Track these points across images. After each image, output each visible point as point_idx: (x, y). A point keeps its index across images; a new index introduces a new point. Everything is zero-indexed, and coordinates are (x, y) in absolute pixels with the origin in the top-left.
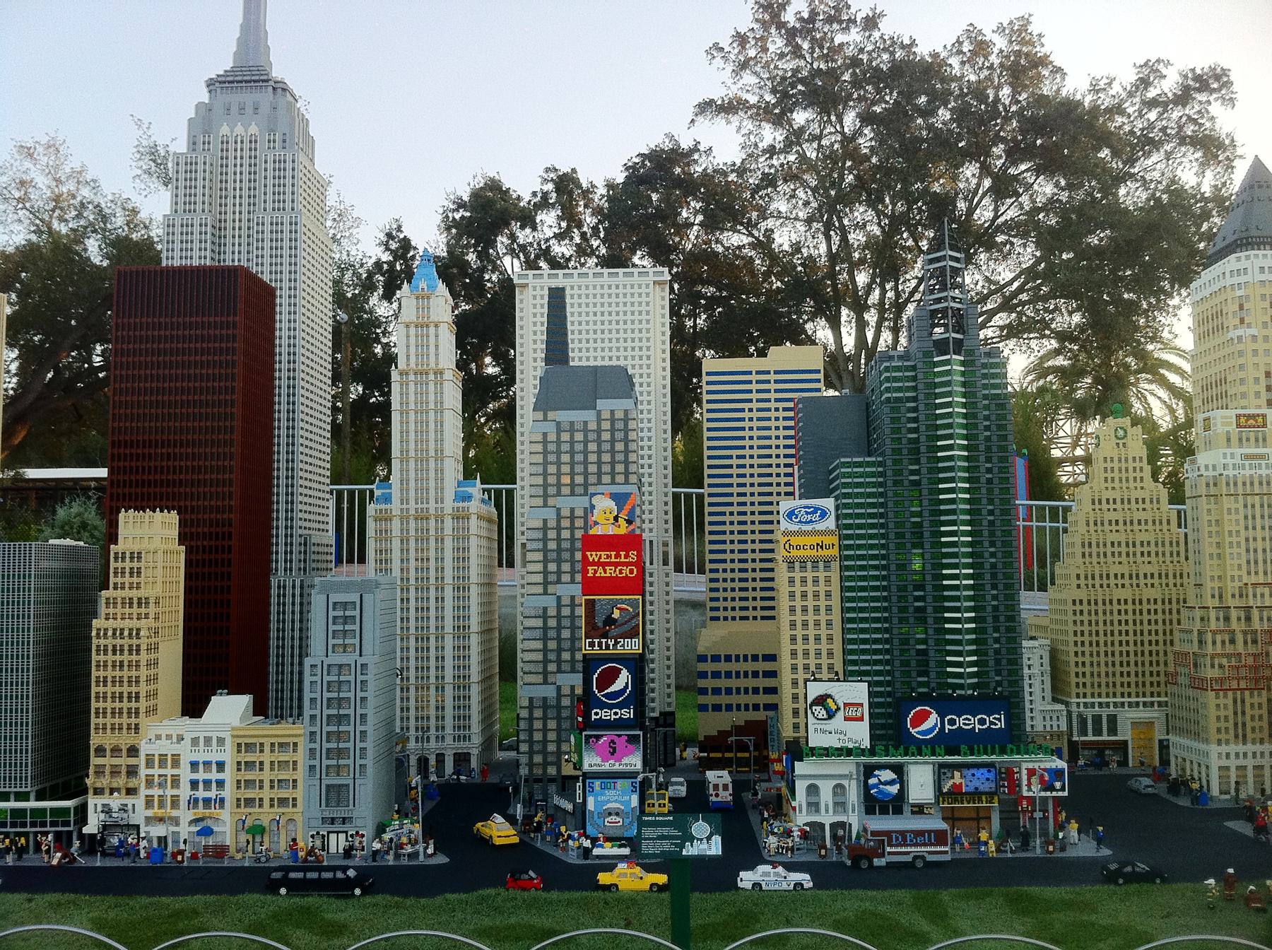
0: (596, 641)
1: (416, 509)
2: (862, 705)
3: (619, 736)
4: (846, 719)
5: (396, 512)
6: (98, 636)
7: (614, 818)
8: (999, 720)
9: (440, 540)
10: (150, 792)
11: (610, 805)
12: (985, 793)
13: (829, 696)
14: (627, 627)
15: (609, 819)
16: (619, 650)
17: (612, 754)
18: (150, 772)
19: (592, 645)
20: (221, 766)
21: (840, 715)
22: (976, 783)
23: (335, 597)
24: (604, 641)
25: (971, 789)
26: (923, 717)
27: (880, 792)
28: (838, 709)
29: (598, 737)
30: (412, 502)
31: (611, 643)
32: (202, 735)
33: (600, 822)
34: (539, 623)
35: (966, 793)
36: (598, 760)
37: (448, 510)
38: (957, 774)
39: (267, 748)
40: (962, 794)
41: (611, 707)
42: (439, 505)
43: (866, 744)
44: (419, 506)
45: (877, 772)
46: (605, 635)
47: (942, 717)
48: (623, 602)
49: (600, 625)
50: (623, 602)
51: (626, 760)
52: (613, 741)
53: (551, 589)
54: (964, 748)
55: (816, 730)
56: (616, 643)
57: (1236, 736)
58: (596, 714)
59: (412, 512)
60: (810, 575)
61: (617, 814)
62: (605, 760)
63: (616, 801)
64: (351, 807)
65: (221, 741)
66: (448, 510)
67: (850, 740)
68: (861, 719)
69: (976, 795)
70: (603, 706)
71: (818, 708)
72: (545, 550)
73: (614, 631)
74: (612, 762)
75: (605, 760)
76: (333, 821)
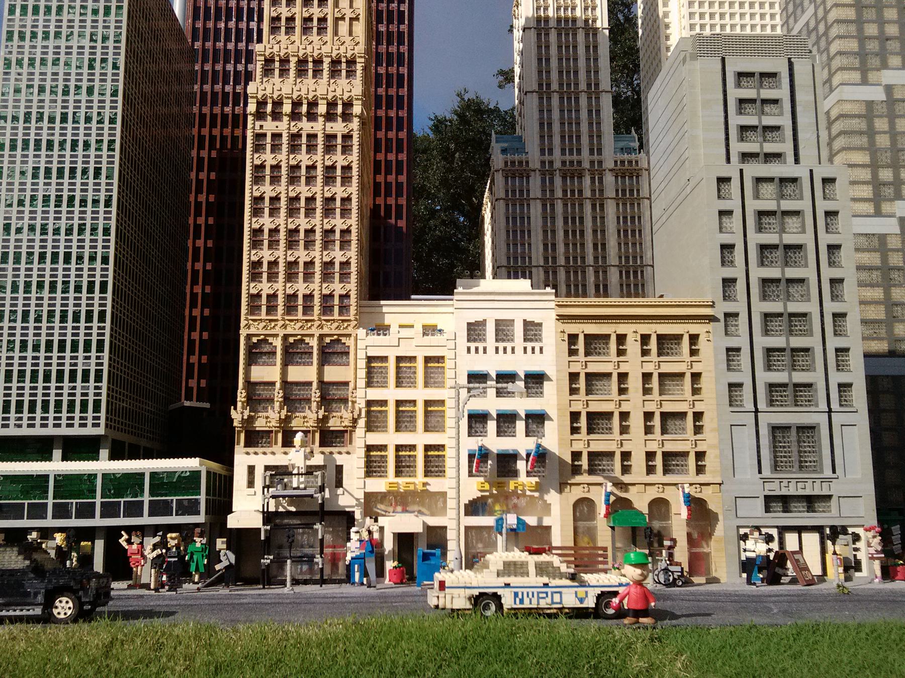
1: (564, 163)
5: (535, 164)
6: (260, 115)
9: (598, 203)
10: (375, 438)
18: (375, 394)
20: (535, 380)
23: (735, 65)
30: (557, 152)
32: (491, 317)
34: (874, 259)
37: (609, 164)
39: (633, 346)
42: (596, 157)
44: (568, 157)
53: (886, 207)
59: (557, 165)
64: (828, 472)
65: (532, 330)
66: (609, 164)
72: (872, 149)
76: (786, 502)
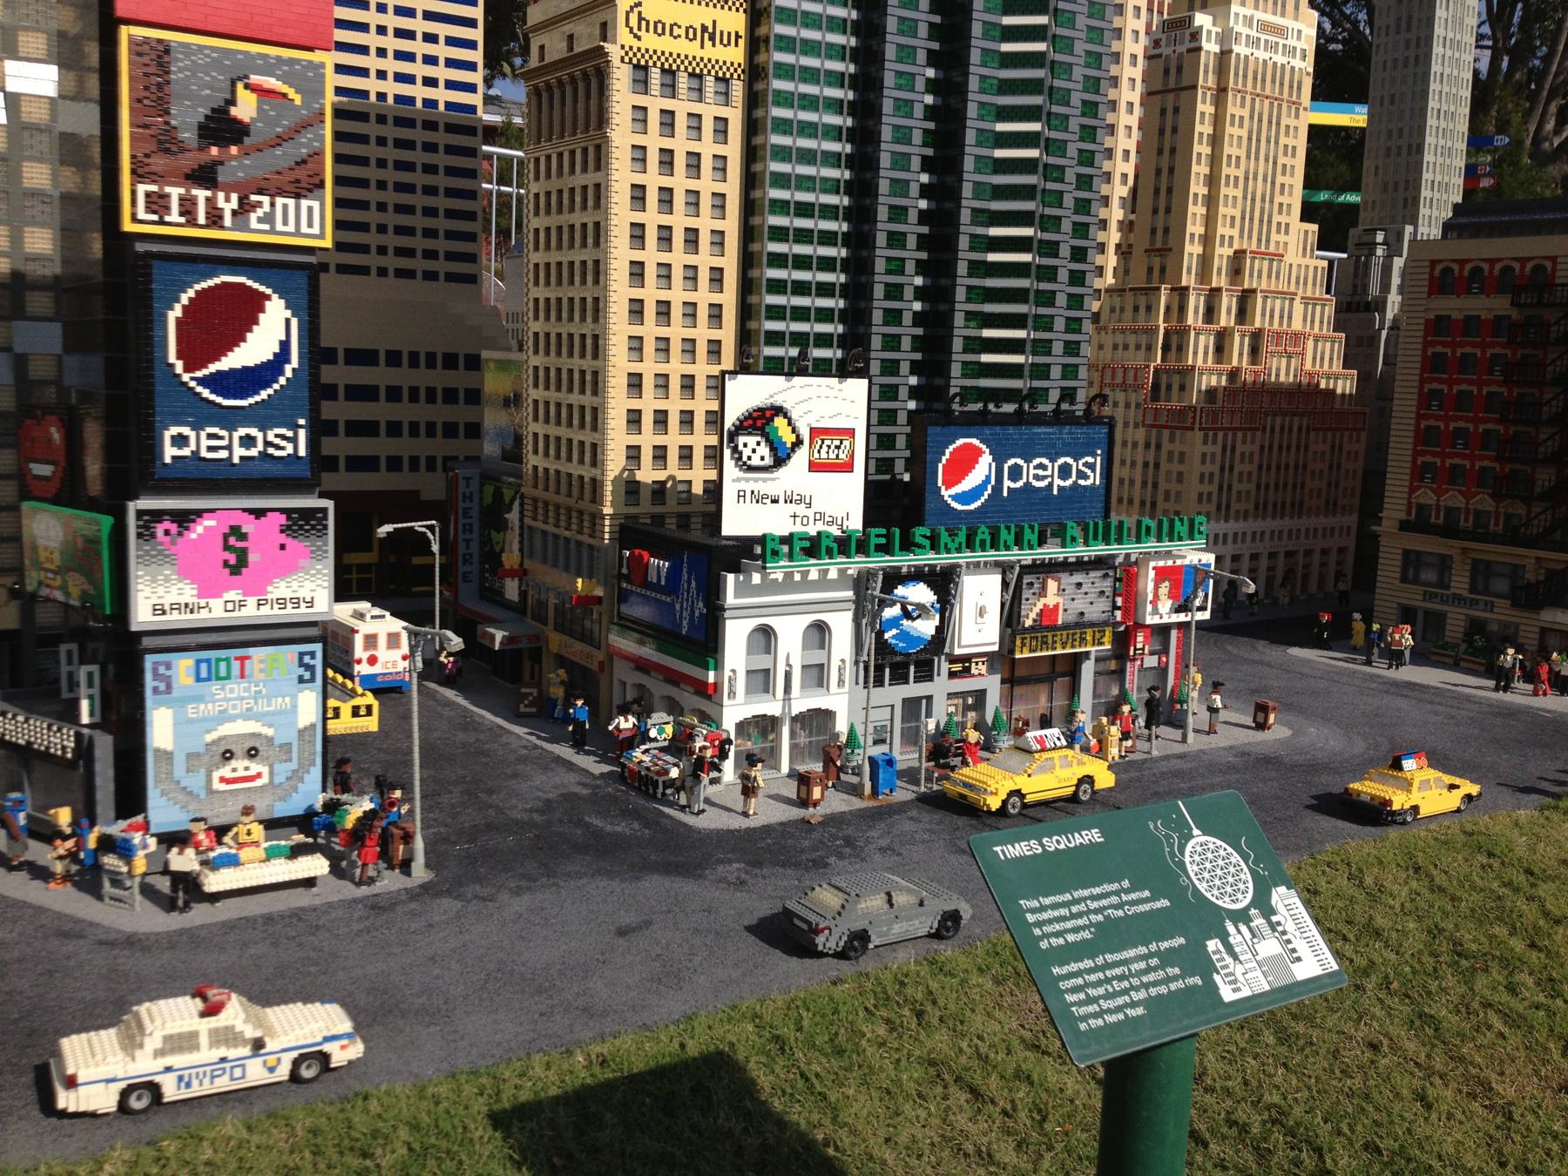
0: (175, 192)
2: (851, 433)
3: (259, 513)
4: (814, 467)
7: (240, 766)
8: (1092, 467)
11: (228, 729)
12: (1092, 625)
13: (778, 411)
14: (282, 156)
15: (226, 771)
16: (256, 230)
17: (236, 570)
19: (157, 203)
21: (801, 457)
22: (1080, 605)
24: (201, 194)
25: (1071, 617)
26: (964, 463)
27: (904, 635)
28: (798, 443)
29: (184, 519)
31: (228, 204)
33: (195, 782)
35: (1066, 627)
36: (186, 592)
38: (1052, 585)
40: (1054, 628)
41: (230, 419)
43: (856, 523)
45: (900, 591)
46: (205, 176)
47: (999, 459)
48: (268, 68)
49: (189, 136)
50: (268, 68)
51: (280, 589)
52: (235, 531)
54: (1073, 530)
55: (741, 495)
56: (245, 208)
57: (1219, 508)
58: (180, 440)
60: (682, 107)
61: (252, 753)
62: (208, 590)
63: (248, 715)
67: (820, 516)
68: (847, 467)
69: (1080, 625)
70: (203, 415)
71: (751, 440)
73: (235, 161)
74: (233, 595)
75: (208, 590)
